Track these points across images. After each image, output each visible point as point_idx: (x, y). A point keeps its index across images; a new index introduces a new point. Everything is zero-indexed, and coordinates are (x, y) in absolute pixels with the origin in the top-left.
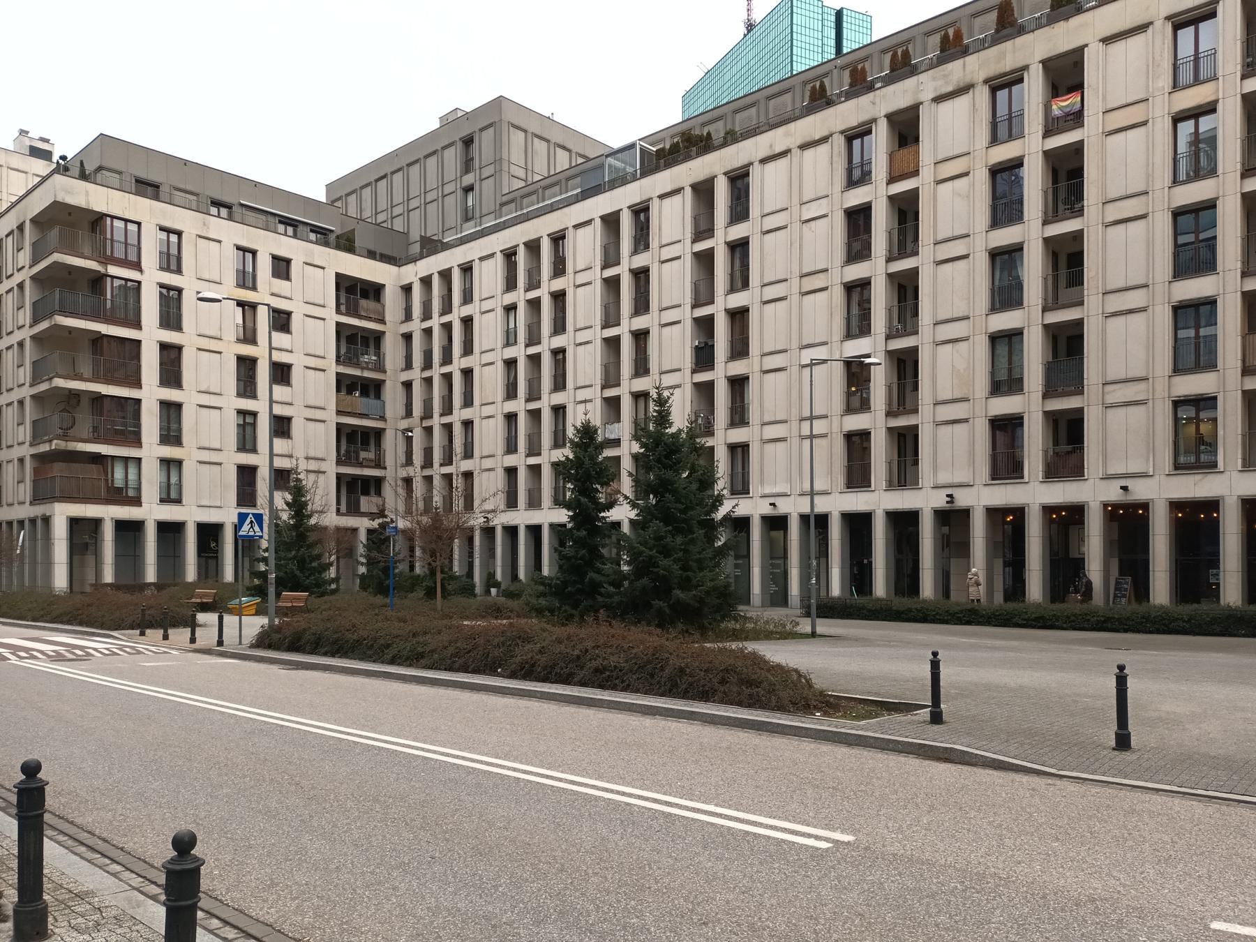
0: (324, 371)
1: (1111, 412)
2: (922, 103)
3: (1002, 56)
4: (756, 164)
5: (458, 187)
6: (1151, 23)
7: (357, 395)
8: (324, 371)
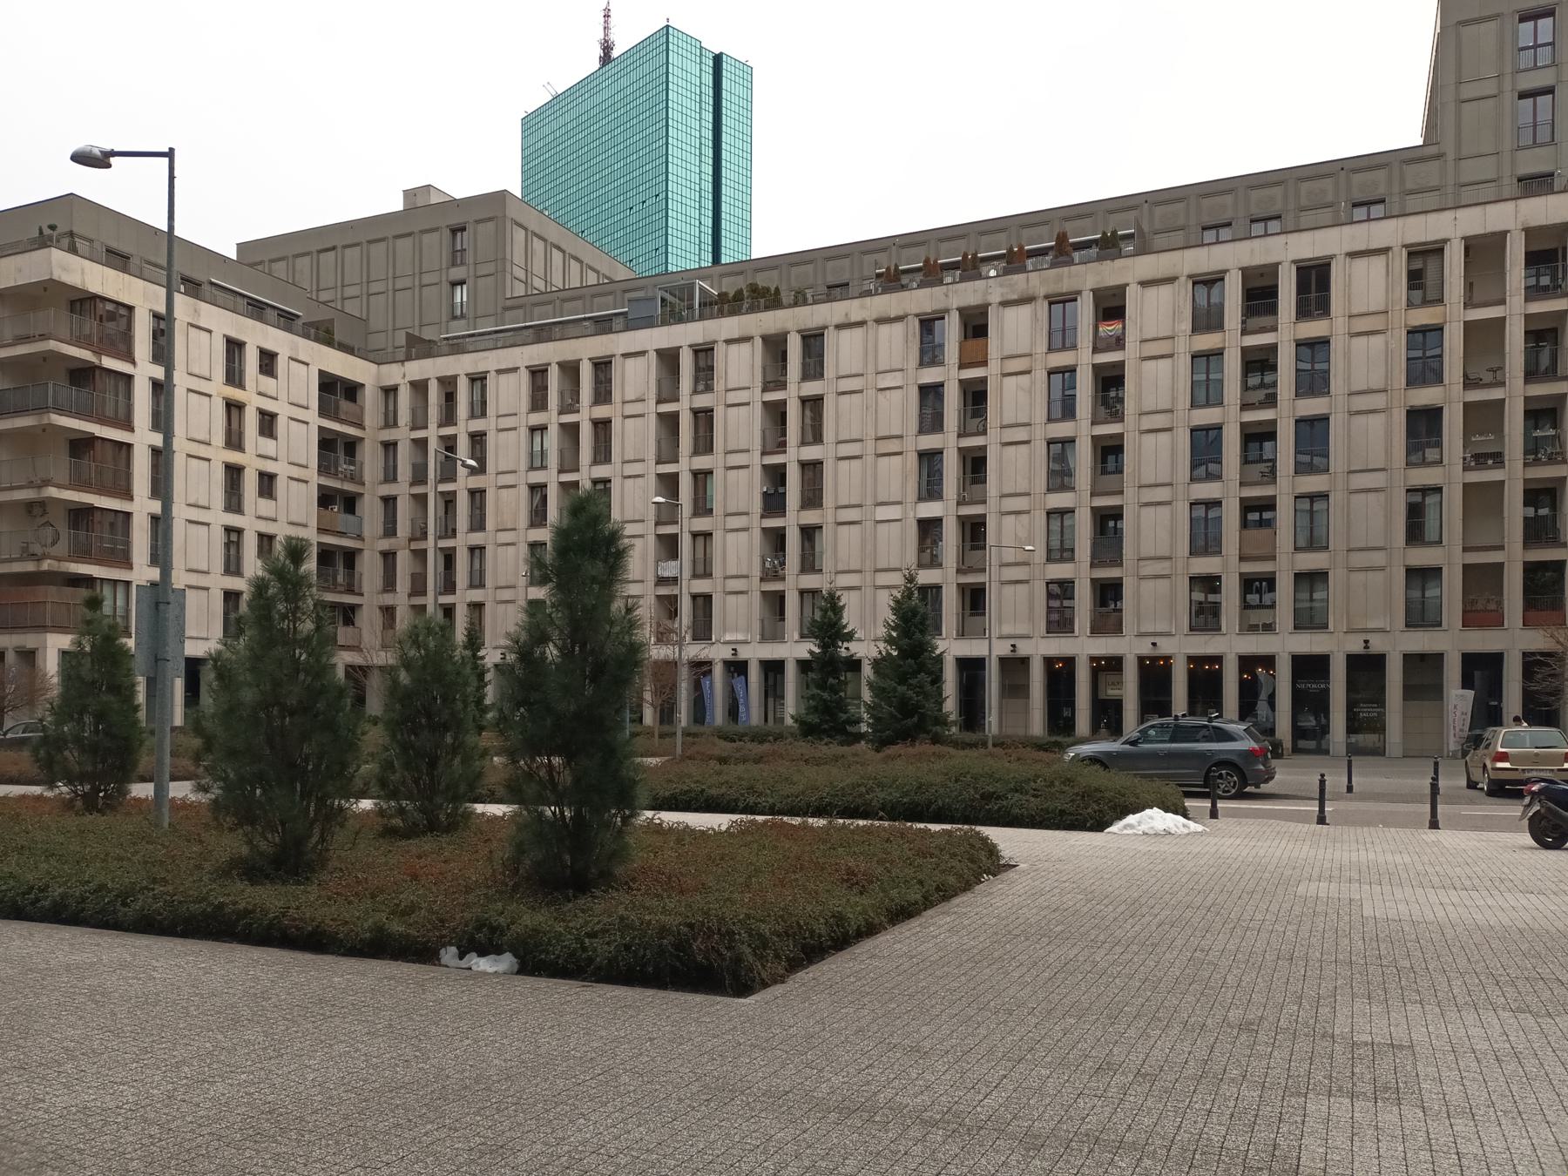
0: (306, 482)
1: (1143, 583)
2: (990, 304)
3: (1060, 278)
4: (831, 328)
5: (444, 279)
6: (1177, 278)
7: (336, 510)
8: (306, 482)
